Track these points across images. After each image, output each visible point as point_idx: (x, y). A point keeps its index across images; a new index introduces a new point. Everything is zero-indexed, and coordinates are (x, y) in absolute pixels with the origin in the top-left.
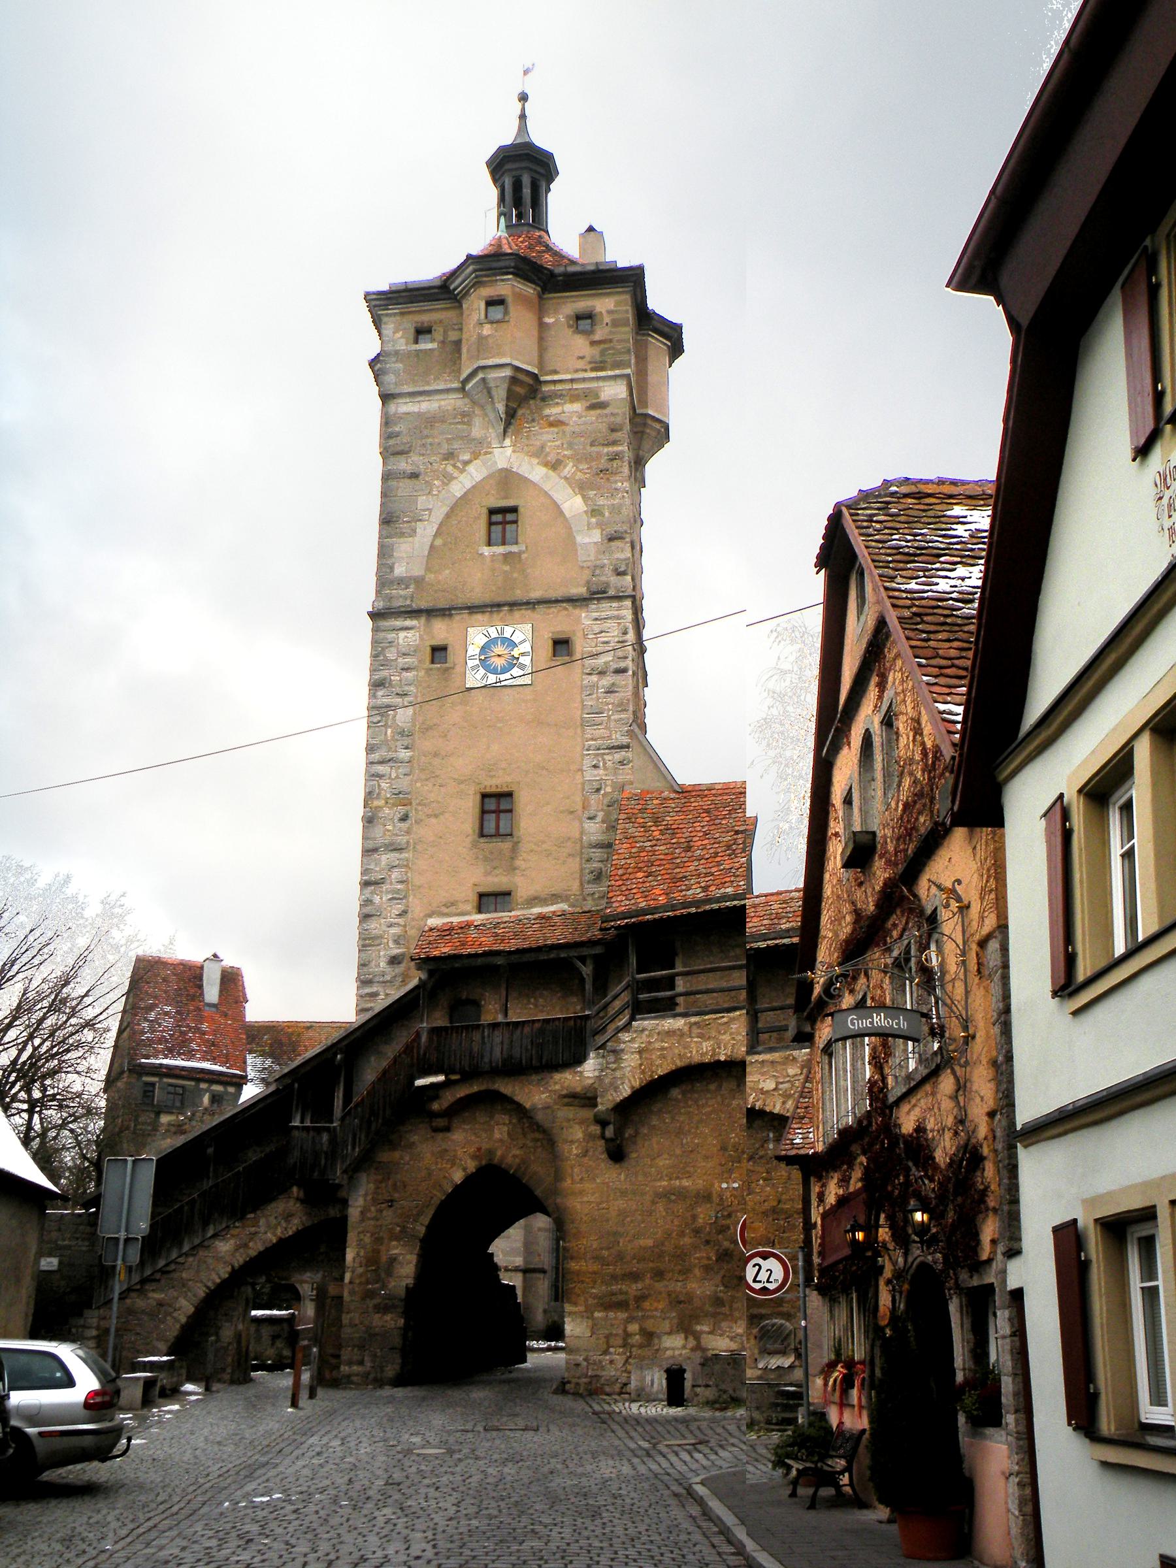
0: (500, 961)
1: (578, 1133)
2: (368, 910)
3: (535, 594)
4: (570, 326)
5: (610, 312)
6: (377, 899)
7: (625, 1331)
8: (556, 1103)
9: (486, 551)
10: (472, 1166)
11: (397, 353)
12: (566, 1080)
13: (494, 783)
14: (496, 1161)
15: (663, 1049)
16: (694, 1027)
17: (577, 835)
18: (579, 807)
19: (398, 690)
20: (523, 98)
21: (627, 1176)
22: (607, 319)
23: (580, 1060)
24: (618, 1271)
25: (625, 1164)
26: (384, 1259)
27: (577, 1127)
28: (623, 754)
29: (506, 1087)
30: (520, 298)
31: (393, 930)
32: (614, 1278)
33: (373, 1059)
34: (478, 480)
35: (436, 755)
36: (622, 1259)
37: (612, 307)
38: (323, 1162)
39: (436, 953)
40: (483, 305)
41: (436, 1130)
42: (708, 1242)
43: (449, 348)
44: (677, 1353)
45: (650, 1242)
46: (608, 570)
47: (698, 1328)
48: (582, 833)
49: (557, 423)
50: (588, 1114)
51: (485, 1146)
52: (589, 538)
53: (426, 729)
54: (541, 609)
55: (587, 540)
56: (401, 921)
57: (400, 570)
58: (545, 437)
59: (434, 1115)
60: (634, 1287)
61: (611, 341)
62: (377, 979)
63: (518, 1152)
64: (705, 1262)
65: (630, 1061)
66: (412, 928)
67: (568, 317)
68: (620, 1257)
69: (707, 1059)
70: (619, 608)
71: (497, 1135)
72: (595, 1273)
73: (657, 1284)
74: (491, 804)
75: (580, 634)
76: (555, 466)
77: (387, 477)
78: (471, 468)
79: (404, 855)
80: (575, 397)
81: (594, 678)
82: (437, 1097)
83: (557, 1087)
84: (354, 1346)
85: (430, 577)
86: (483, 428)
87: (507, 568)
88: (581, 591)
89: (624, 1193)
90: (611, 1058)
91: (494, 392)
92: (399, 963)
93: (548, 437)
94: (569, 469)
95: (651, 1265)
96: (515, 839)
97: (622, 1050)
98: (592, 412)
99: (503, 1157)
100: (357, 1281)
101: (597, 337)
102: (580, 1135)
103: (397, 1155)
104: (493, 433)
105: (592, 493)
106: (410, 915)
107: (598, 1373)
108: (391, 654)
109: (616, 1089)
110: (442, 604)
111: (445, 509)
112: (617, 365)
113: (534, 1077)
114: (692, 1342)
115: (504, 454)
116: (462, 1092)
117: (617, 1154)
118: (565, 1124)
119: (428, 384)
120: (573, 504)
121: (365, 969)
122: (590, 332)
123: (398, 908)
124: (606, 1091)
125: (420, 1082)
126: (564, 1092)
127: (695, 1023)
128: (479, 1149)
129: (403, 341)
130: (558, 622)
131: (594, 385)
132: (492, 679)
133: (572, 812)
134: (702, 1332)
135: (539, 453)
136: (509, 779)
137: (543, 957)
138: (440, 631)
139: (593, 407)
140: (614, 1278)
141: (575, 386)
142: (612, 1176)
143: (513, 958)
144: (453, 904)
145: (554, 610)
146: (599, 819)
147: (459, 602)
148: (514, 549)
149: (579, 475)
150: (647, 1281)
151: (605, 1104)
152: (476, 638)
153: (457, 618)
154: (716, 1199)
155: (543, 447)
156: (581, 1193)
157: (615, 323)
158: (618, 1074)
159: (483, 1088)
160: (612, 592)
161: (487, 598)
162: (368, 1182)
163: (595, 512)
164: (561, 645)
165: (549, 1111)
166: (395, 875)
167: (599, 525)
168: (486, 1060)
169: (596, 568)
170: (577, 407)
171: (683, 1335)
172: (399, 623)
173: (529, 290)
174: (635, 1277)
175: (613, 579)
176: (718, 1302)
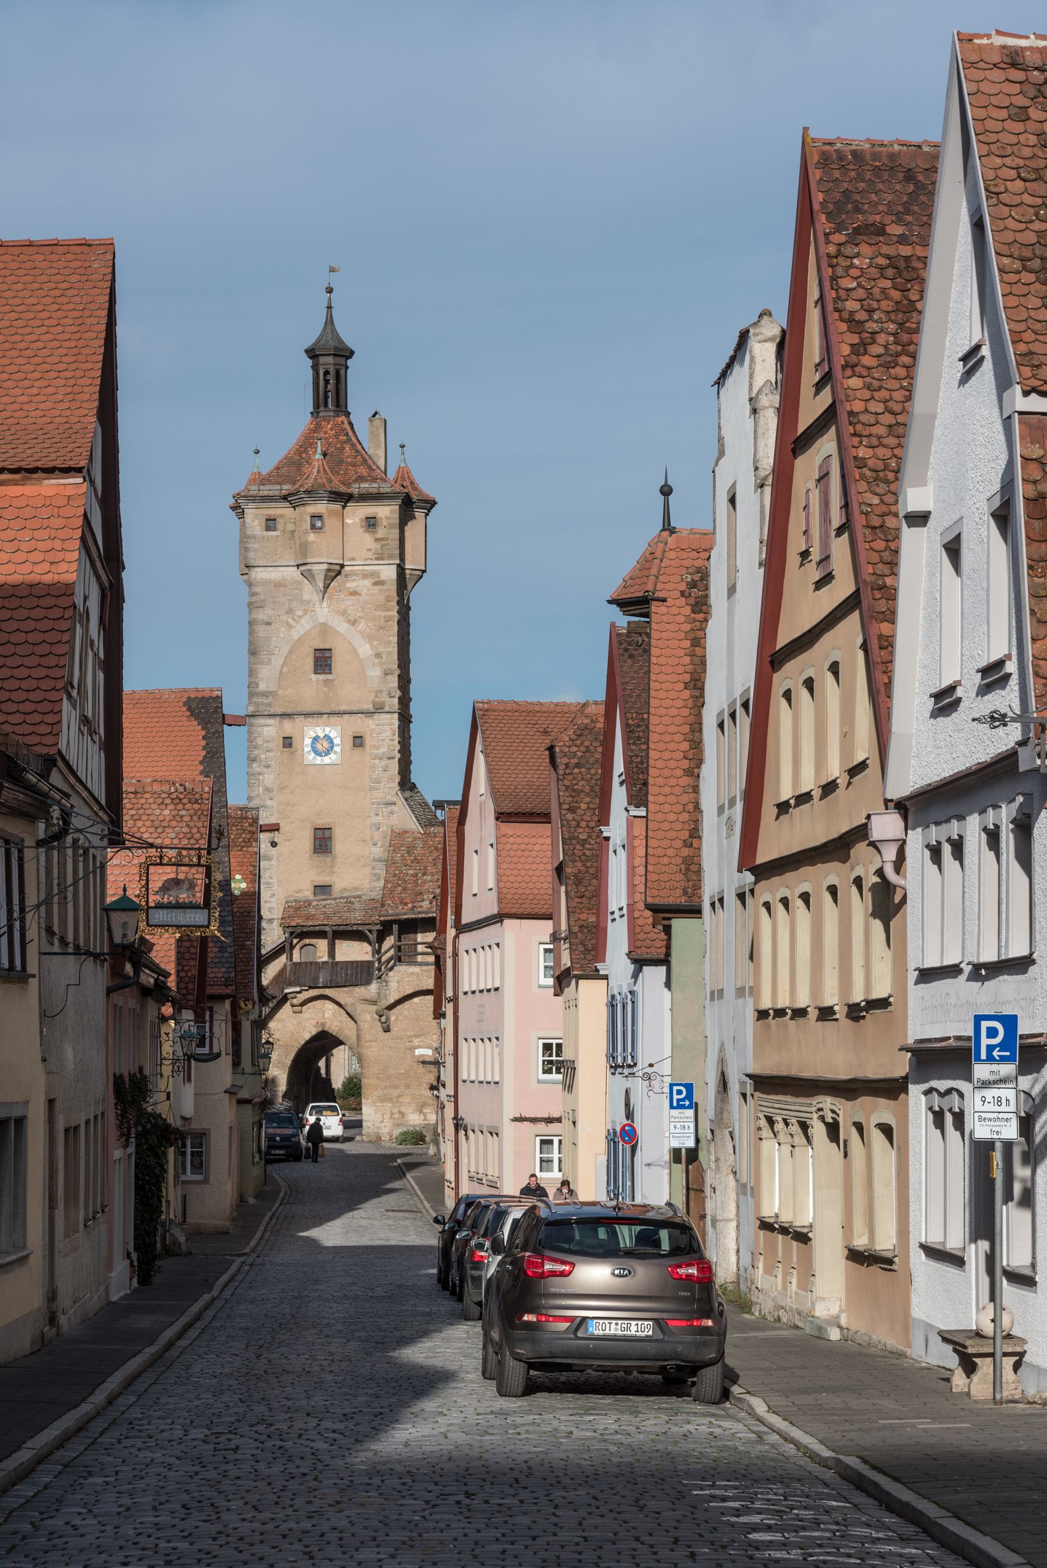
0: (327, 929)
1: (368, 1017)
3: (342, 708)
4: (362, 527)
5: (387, 518)
9: (314, 677)
10: (314, 1032)
11: (254, 537)
13: (322, 822)
18: (368, 838)
19: (264, 763)
20: (330, 290)
22: (385, 523)
23: (368, 983)
25: (391, 1033)
28: (393, 807)
30: (331, 513)
32: (386, 1087)
34: (308, 628)
35: (288, 804)
37: (388, 514)
39: (294, 924)
40: (309, 519)
43: (287, 536)
46: (385, 694)
49: (355, 593)
50: (374, 1008)
52: (375, 673)
53: (282, 788)
54: (346, 717)
55: (372, 674)
57: (262, 687)
58: (348, 603)
61: (387, 539)
65: (393, 985)
67: (361, 520)
68: (389, 1077)
70: (392, 719)
71: (327, 1015)
74: (320, 834)
75: (368, 734)
76: (354, 623)
77: (251, 623)
78: (303, 621)
80: (365, 576)
81: (377, 761)
85: (280, 692)
86: (309, 592)
87: (326, 689)
88: (370, 707)
89: (391, 1048)
91: (317, 577)
93: (349, 603)
94: (362, 626)
98: (377, 588)
101: (379, 536)
104: (316, 598)
105: (376, 642)
108: (259, 741)
110: (289, 711)
111: (288, 648)
112: (390, 557)
115: (323, 612)
117: (387, 1030)
119: (275, 561)
120: (365, 650)
122: (375, 532)
125: (286, 991)
129: (258, 528)
130: (359, 724)
131: (378, 567)
132: (318, 760)
135: (344, 613)
136: (329, 820)
137: (349, 928)
138: (288, 727)
139: (376, 584)
140: (386, 1087)
141: (366, 568)
143: (335, 928)
145: (353, 717)
146: (380, 844)
147: (299, 709)
148: (329, 677)
149: (368, 630)
152: (310, 731)
153: (297, 720)
155: (345, 611)
156: (370, 1047)
157: (390, 526)
160: (387, 709)
161: (314, 709)
163: (378, 655)
164: (358, 741)
167: (380, 664)
169: (378, 692)
170: (367, 582)
172: (261, 721)
173: (337, 507)
174: (396, 1087)
175: (388, 699)
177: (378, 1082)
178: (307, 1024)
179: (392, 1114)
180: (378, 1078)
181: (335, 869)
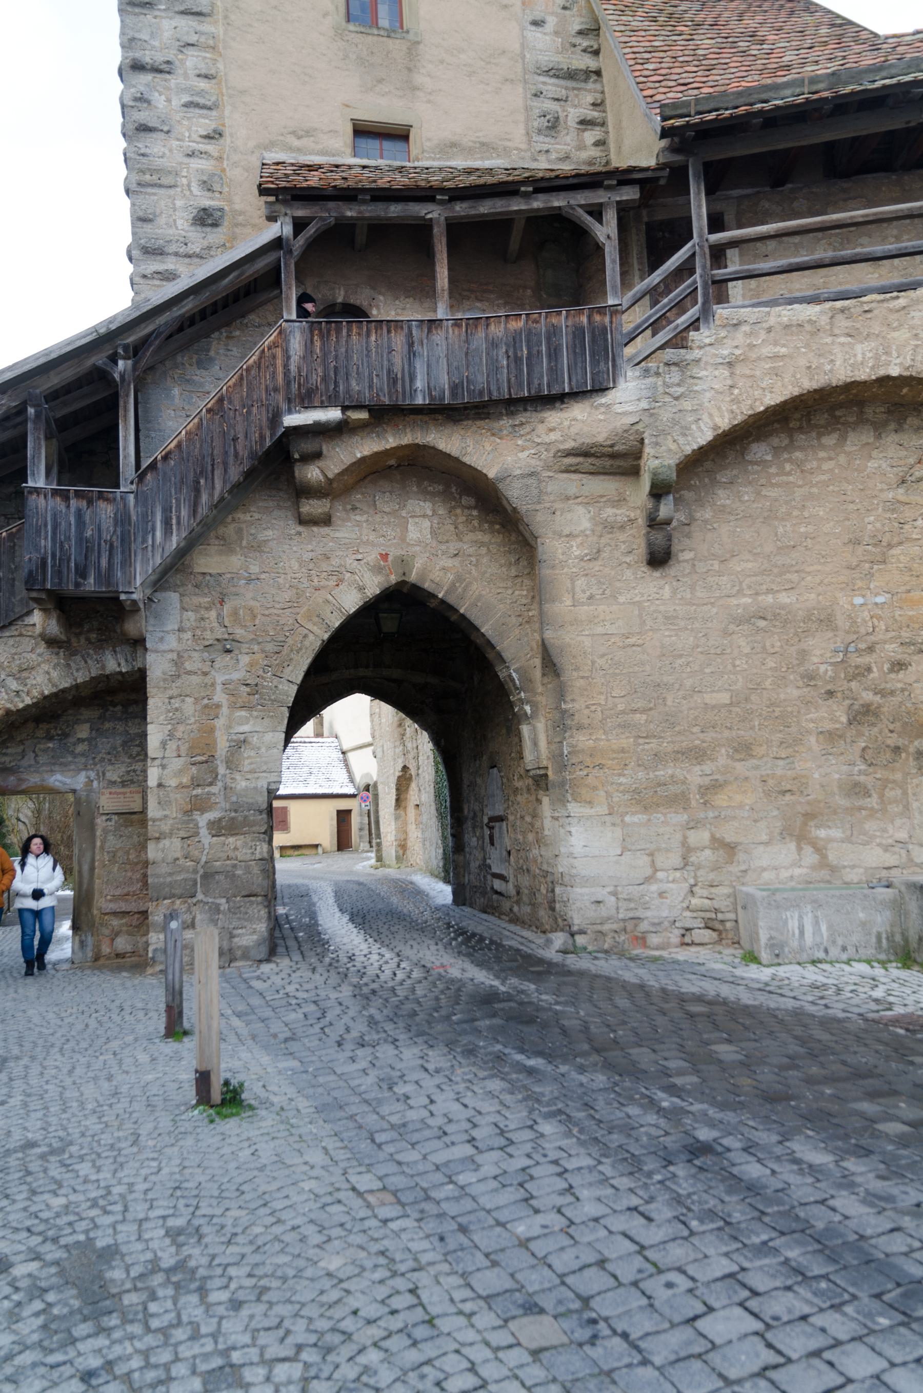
0: (434, 212)
2: (143, 116)
6: (159, 101)
7: (684, 843)
8: (548, 468)
10: (373, 586)
12: (580, 422)
14: (413, 578)
15: (776, 357)
16: (840, 317)
17: (517, 46)
21: (674, 591)
24: (667, 747)
25: (673, 570)
26: (222, 745)
27: (581, 510)
29: (451, 442)
31: (197, 164)
33: (176, 391)
36: (673, 725)
38: (104, 562)
41: (303, 521)
42: (830, 693)
44: (784, 874)
45: (725, 698)
47: (822, 833)
48: (523, 46)
51: (394, 553)
56: (210, 148)
59: (303, 492)
60: (697, 769)
62: (172, 248)
63: (449, 563)
64: (828, 726)
66: (235, 164)
69: (863, 375)
71: (413, 533)
72: (623, 751)
73: (738, 765)
79: (207, 27)
82: (318, 455)
83: (553, 436)
84: (172, 896)
89: (670, 619)
90: (674, 376)
92: (215, 225)
95: (727, 733)
96: (411, 36)
97: (698, 361)
99: (423, 575)
100: (173, 783)
102: (586, 524)
103: (235, 561)
106: (227, 140)
107: (638, 914)
109: (685, 431)
113: (505, 423)
114: (810, 857)
116: (365, 447)
117: (659, 558)
118: (557, 505)
121: (148, 227)
123: (204, 123)
124: (664, 433)
125: (292, 420)
126: (570, 445)
127: (842, 311)
128: (385, 557)
133: (506, 6)
134: (830, 840)
142: (655, 587)
143: (461, 209)
144: (308, 133)
150: (722, 760)
151: (660, 458)
154: (841, 621)
158: (687, 405)
159: (407, 439)
162: (184, 609)
165: (531, 481)
166: (192, 61)
168: (419, 384)
171: (793, 846)
174: (699, 755)
176: (857, 789)
177: (625, 741)
178: (350, 562)
179: (687, 850)
180: (624, 726)
181: (419, 79)
